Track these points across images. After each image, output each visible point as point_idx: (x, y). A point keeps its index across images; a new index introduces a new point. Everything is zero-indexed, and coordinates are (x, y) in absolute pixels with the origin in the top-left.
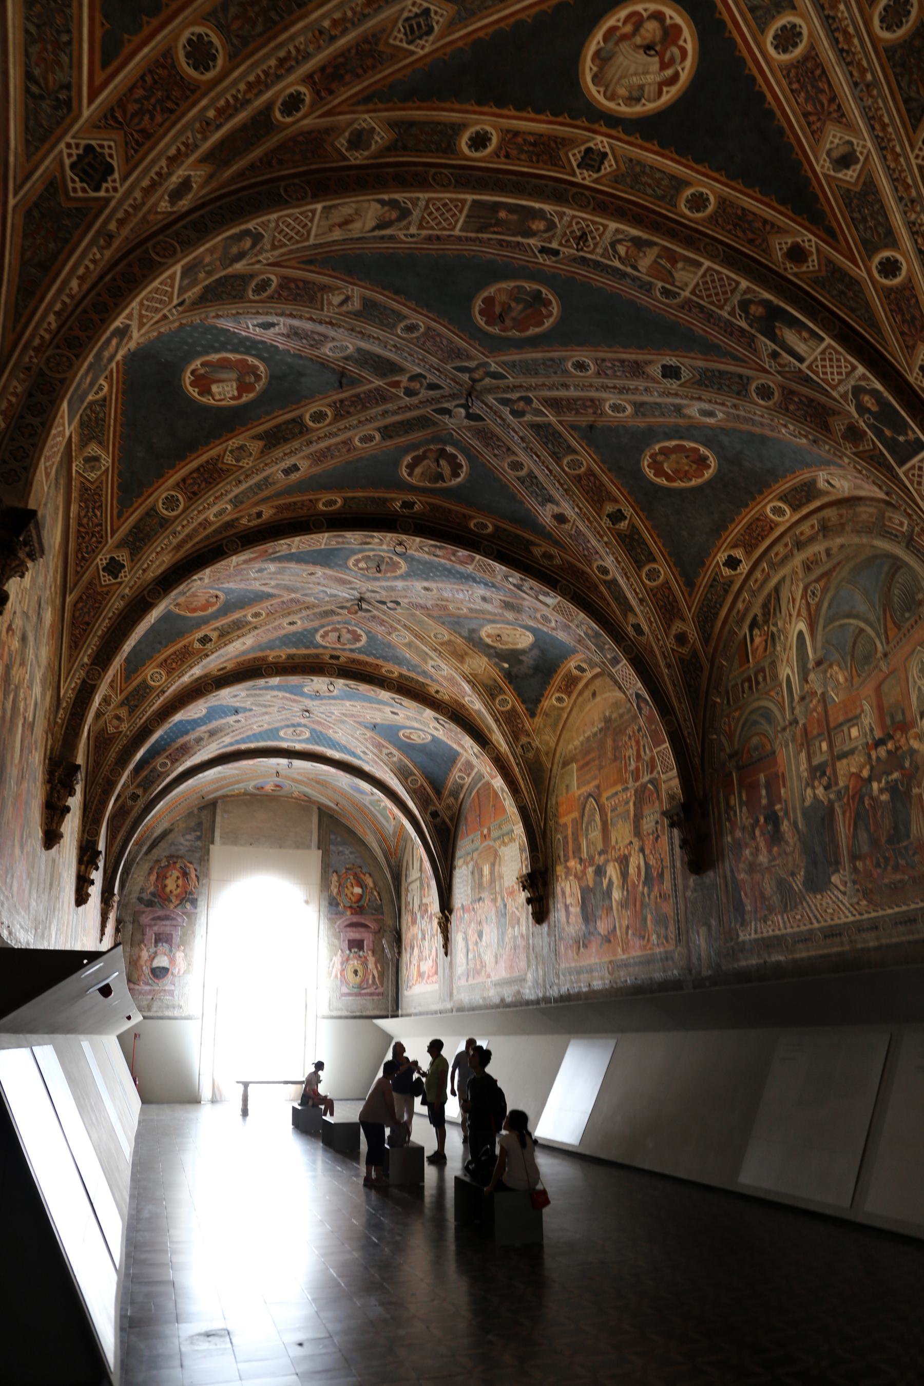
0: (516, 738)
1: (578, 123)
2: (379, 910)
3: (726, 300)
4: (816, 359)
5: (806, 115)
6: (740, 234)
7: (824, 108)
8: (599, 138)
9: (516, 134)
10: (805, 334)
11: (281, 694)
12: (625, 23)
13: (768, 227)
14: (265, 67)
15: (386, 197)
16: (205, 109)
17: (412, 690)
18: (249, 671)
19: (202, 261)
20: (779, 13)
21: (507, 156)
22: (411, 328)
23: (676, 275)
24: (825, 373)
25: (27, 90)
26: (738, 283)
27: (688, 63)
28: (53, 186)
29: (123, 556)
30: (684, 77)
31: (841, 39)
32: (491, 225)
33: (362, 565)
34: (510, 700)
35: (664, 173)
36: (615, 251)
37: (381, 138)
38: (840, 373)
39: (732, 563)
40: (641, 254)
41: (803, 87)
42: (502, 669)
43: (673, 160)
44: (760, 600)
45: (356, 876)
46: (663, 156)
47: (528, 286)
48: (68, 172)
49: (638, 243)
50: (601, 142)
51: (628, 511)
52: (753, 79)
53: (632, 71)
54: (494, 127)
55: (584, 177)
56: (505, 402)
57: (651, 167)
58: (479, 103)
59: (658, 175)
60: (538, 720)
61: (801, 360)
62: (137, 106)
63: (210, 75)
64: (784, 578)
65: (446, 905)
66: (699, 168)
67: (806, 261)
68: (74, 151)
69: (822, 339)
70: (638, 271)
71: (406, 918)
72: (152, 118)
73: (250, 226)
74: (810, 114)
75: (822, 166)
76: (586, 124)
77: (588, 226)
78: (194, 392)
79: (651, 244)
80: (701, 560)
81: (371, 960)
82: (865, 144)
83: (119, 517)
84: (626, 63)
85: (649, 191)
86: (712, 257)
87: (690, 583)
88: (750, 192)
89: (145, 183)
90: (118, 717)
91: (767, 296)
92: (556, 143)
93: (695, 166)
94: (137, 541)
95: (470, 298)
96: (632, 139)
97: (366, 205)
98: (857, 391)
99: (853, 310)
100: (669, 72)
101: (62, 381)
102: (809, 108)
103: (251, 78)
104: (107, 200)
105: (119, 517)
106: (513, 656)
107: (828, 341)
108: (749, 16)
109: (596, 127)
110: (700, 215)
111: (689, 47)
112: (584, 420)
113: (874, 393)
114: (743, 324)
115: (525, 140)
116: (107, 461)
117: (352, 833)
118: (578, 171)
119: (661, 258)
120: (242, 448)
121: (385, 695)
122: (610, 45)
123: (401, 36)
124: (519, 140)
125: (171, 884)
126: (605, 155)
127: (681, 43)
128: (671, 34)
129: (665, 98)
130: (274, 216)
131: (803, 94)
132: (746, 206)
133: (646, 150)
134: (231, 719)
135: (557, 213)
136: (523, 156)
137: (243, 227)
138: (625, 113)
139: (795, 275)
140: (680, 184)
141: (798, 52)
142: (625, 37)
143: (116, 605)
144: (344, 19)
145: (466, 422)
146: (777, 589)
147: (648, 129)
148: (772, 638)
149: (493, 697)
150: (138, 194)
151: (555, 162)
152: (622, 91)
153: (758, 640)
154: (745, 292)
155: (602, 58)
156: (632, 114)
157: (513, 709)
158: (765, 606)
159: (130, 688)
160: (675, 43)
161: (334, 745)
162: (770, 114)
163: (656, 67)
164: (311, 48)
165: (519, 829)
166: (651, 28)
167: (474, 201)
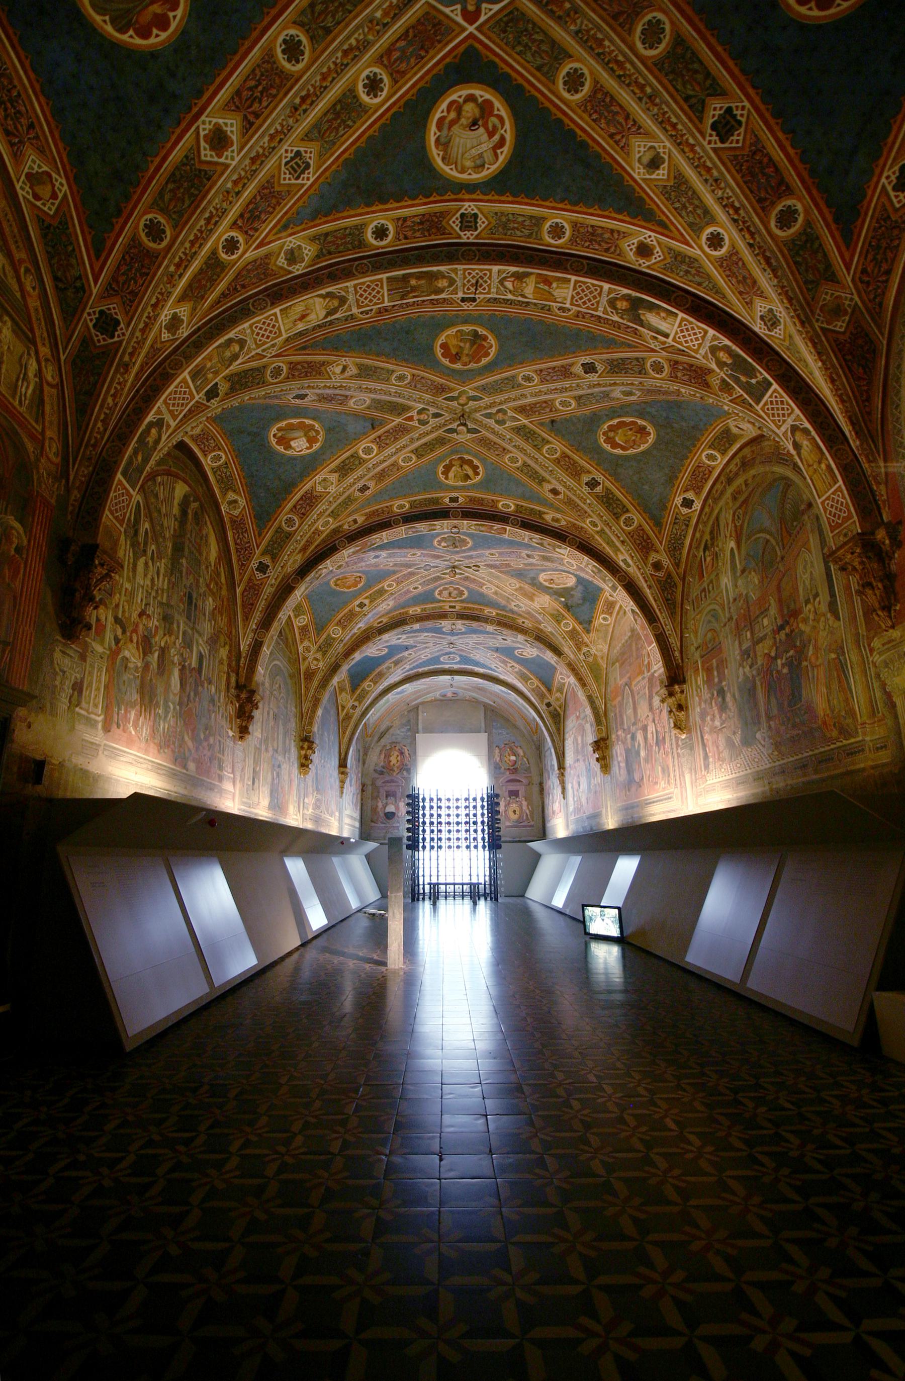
0: (579, 649)
2: (528, 770)
3: (598, 303)
4: (677, 333)
5: (612, 136)
7: (624, 127)
8: (467, 204)
9: (405, 219)
10: (663, 314)
11: (430, 634)
12: (449, 111)
13: (616, 235)
14: (198, 227)
15: (323, 292)
16: (167, 266)
17: (507, 623)
18: (397, 622)
19: (205, 366)
21: (406, 238)
22: (401, 378)
23: (555, 293)
25: (57, 287)
26: (601, 287)
28: (86, 341)
29: (267, 560)
30: (508, 137)
31: (615, 68)
32: (409, 293)
33: (443, 544)
34: (570, 623)
36: (505, 287)
37: (309, 251)
39: (687, 503)
41: (601, 115)
42: (561, 602)
43: (526, 204)
44: (708, 529)
45: (511, 749)
47: (467, 328)
48: (93, 331)
49: (519, 277)
50: (469, 207)
51: (600, 478)
53: (469, 146)
54: (387, 219)
55: (468, 237)
56: (489, 416)
59: (520, 219)
60: (593, 635)
62: (125, 278)
63: (164, 244)
64: (721, 509)
65: (561, 767)
66: (547, 204)
67: (653, 254)
68: (93, 317)
69: (676, 315)
71: (546, 775)
72: (136, 283)
73: (231, 335)
75: (639, 173)
76: (453, 197)
78: (281, 449)
79: (527, 275)
80: (663, 505)
81: (525, 803)
82: (665, 145)
83: (260, 535)
85: (519, 233)
86: (576, 272)
87: (658, 523)
89: (141, 325)
90: (316, 659)
91: (626, 291)
94: (274, 550)
95: (431, 348)
97: (311, 301)
98: (714, 350)
99: (700, 284)
100: (496, 138)
101: (115, 462)
102: (613, 130)
103: (192, 237)
104: (121, 342)
105: (260, 535)
106: (565, 592)
107: (681, 315)
108: (538, 74)
109: (460, 196)
111: (503, 113)
112: (547, 417)
113: (726, 349)
114: (616, 318)
116: (242, 502)
117: (507, 720)
118: (462, 234)
120: (325, 480)
121: (490, 628)
122: (445, 132)
123: (287, 176)
124: (409, 223)
125: (393, 760)
127: (496, 112)
128: (486, 108)
129: (501, 158)
130: (246, 325)
134: (406, 654)
135: (451, 270)
136: (418, 234)
137: (226, 337)
140: (538, 221)
141: (586, 89)
143: (268, 591)
144: (240, 178)
145: (469, 436)
146: (717, 519)
147: (500, 185)
148: (716, 556)
149: (558, 622)
150: (138, 334)
152: (468, 164)
153: (708, 559)
154: (609, 293)
155: (444, 144)
157: (574, 629)
158: (711, 532)
159: (321, 641)
160: (491, 114)
161: (477, 664)
162: (583, 145)
164: (225, 205)
165: (588, 711)
166: (470, 109)
167: (388, 278)
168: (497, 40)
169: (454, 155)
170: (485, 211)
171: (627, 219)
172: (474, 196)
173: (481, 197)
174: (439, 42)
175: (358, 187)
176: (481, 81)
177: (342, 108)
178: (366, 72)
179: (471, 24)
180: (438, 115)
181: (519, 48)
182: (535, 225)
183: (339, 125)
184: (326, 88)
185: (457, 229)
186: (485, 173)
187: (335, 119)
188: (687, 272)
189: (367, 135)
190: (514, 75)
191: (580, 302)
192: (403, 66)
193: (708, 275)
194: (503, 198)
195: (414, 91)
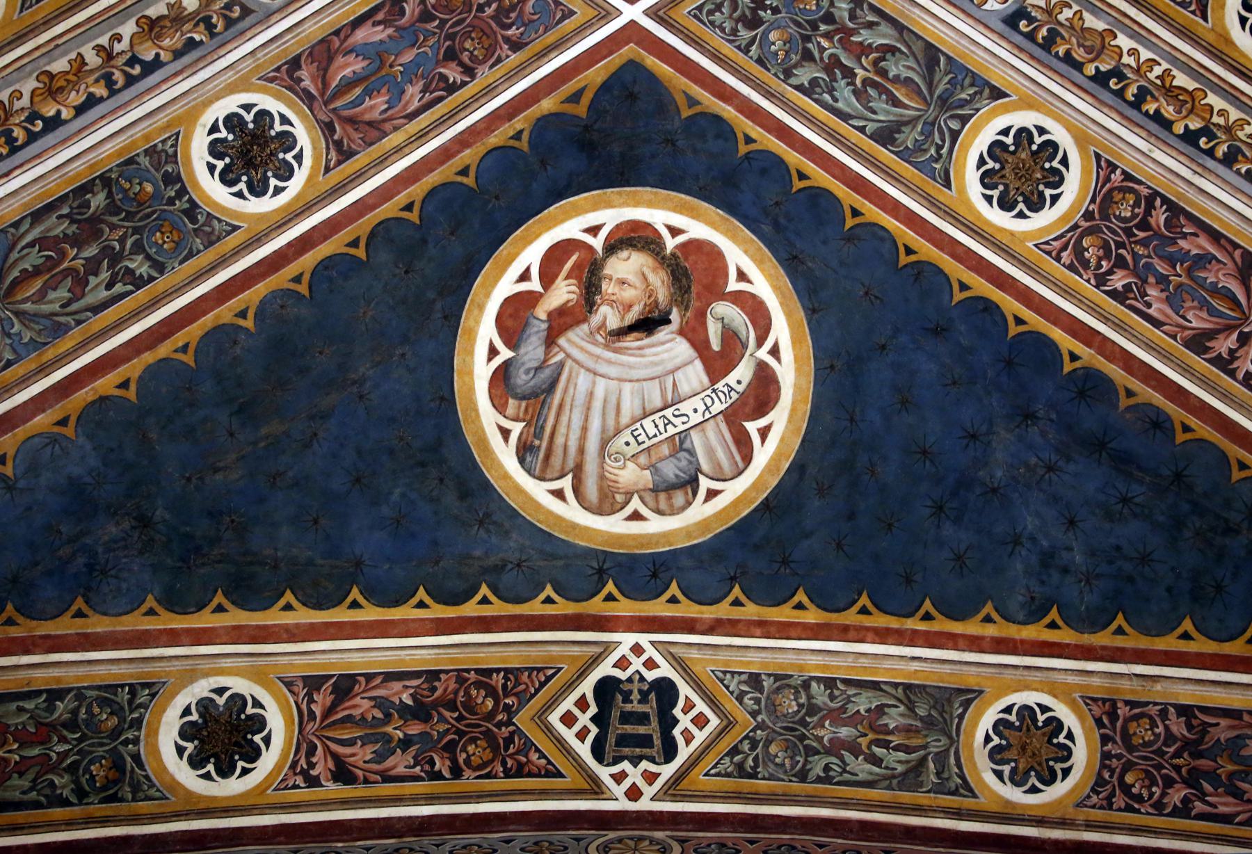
1: (535, 607)
5: (1198, 343)
9: (345, 686)
12: (548, 278)
20: (964, 120)
21: (343, 774)
27: (781, 330)
30: (792, 374)
31: (1169, 111)
41: (1142, 274)
50: (633, 653)
52: (989, 307)
53: (629, 407)
54: (258, 676)
57: (830, 683)
58: (176, 602)
74: (1210, 334)
76: (564, 607)
84: (601, 385)
92: (491, 692)
96: (723, 610)
100: (742, 374)
102: (1197, 321)
108: (884, 154)
109: (596, 606)
111: (762, 287)
115: (380, 703)
122: (533, 350)
124: (361, 705)
126: (665, 690)
127: (733, 285)
129: (763, 455)
131: (1153, 292)
132: (1187, 695)
133: (785, 630)
136: (400, 763)
138: (665, 536)
141: (1074, 188)
142: (562, 320)
147: (759, 559)
151: (517, 760)
152: (630, 475)
155: (525, 392)
156: (687, 532)
160: (717, 291)
162: (1091, 385)
163: (695, 374)
166: (629, 274)
168: (728, 49)
169: (568, 436)
170: (705, 666)
173: (688, 609)
174: (516, 46)
175: (144, 522)
176: (672, 179)
177: (112, 208)
178: (230, 104)
179: (633, 23)
180: (506, 287)
181: (804, 75)
183: (93, 267)
184: (54, 123)
185: (584, 750)
186: (700, 511)
187: (78, 242)
189: (207, 321)
190: (793, 158)
192: (376, 105)
194: (783, 614)
195: (417, 191)
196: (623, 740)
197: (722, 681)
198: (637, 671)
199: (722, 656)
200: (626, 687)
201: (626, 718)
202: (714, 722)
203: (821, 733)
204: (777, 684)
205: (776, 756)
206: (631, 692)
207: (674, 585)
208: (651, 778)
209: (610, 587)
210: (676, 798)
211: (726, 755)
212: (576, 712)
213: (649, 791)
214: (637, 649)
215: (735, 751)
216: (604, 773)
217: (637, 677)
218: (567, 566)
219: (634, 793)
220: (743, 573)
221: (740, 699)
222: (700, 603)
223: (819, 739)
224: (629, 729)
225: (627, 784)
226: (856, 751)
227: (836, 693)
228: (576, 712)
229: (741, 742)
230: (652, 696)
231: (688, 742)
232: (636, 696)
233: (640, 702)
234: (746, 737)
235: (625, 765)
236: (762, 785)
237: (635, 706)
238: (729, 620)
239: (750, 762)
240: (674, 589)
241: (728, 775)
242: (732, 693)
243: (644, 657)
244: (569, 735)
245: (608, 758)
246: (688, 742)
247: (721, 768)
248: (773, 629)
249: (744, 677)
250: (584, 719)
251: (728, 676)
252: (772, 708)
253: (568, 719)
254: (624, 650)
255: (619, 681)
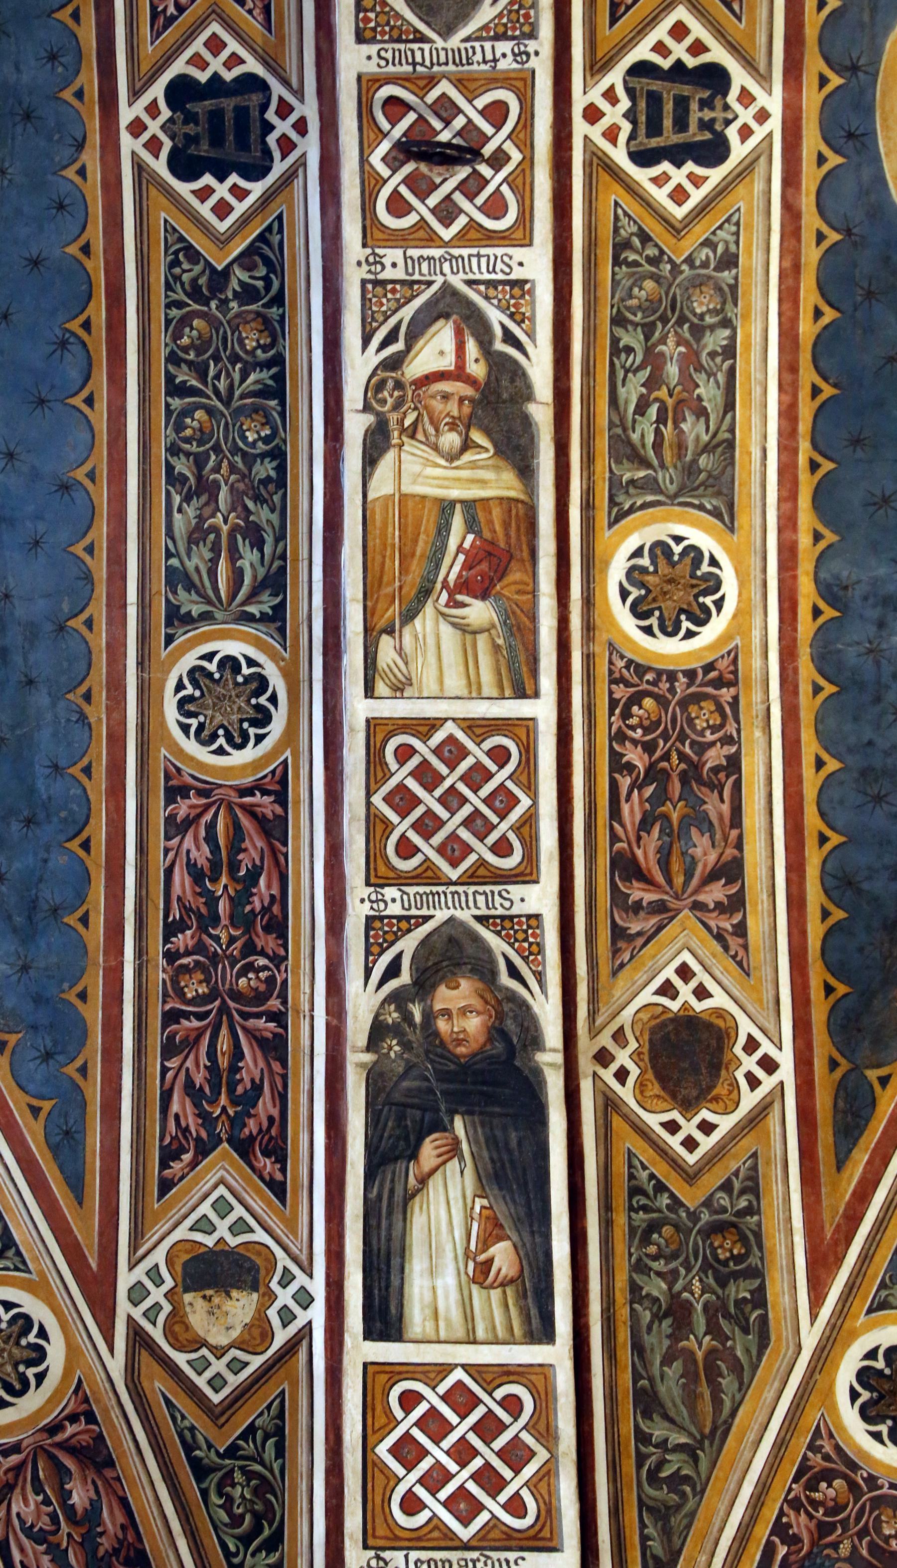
3: (427, 875)
4: (434, 1373)
6: (632, 812)
8: (773, 102)
10: (503, 1256)
13: (716, 893)
23: (426, 621)
24: (409, 1451)
26: (527, 874)
35: (729, 406)
36: (417, 329)
38: (464, 1505)
40: (451, 439)
43: (789, 414)
46: (789, 367)
49: (496, 408)
50: (759, 110)
57: (729, 351)
59: (708, 392)
61: (384, 1321)
67: (688, 1106)
70: (370, 461)
77: (498, 160)
79: (516, 451)
85: (632, 391)
88: (810, 746)
93: (804, 501)
96: (811, 221)
99: (648, 1402)
109: (814, 63)
110: (628, 623)
118: (615, 77)
119: (471, 525)
126: (713, 151)
133: (789, 296)
139: (609, 1104)
140: (711, 486)
154: (503, 923)
170: (742, 200)
171: (815, 931)
172: (811, 140)
182: (691, 470)
185: (642, 52)
188: (677, 1312)
191: (401, 775)
193: (721, 1431)
194: (809, 294)
196: (654, 99)
197: (728, 220)
198: (736, 117)
199: (758, 220)
200: (718, 103)
201: (682, 103)
202: (679, 212)
203: (671, 341)
204: (726, 289)
205: (641, 289)
206: (712, 109)
207: (839, 160)
208: (611, 135)
209: (836, 81)
210: (588, 165)
211: (640, 228)
212: (688, 41)
213: (596, 133)
214: (762, 116)
215: (645, 238)
216: (615, 77)
217: (730, 117)
218: (862, 25)
219: (592, 114)
220: (855, 244)
221: (707, 243)
222: (819, 193)
223: (663, 340)
224: (668, 107)
225: (604, 105)
226: (652, 383)
227: (719, 360)
228: (688, 41)
229: (656, 245)
230: (708, 136)
231: (654, 180)
232: (707, 115)
233: (701, 120)
234: (662, 252)
235: (625, 103)
236: (606, 270)
237: (695, 114)
238: (799, 229)
239: (632, 257)
240: (834, 160)
241: (616, 230)
242: (714, 233)
243: (754, 125)
244: (661, 32)
245: (634, 82)
246: (654, 180)
247: (625, 221)
248: (790, 282)
249: (733, 248)
250: (679, 51)
251: (734, 229)
252: (698, 283)
253: (679, 31)
254: (763, 100)
255: (725, 94)
